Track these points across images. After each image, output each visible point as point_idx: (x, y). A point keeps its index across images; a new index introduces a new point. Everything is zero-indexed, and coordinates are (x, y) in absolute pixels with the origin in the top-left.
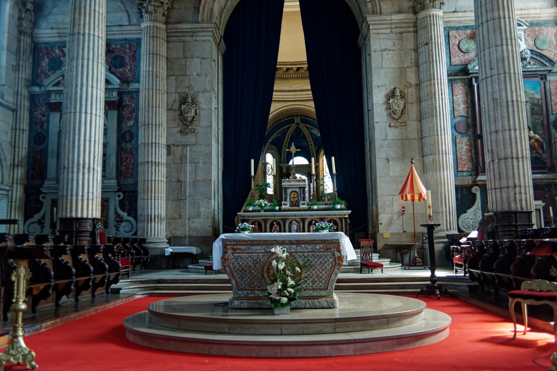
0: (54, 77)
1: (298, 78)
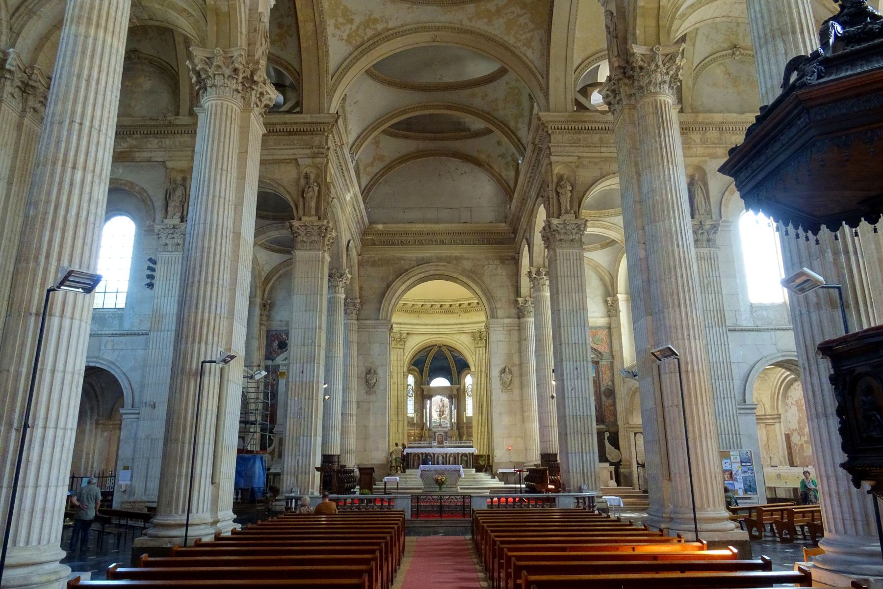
0: (283, 356)
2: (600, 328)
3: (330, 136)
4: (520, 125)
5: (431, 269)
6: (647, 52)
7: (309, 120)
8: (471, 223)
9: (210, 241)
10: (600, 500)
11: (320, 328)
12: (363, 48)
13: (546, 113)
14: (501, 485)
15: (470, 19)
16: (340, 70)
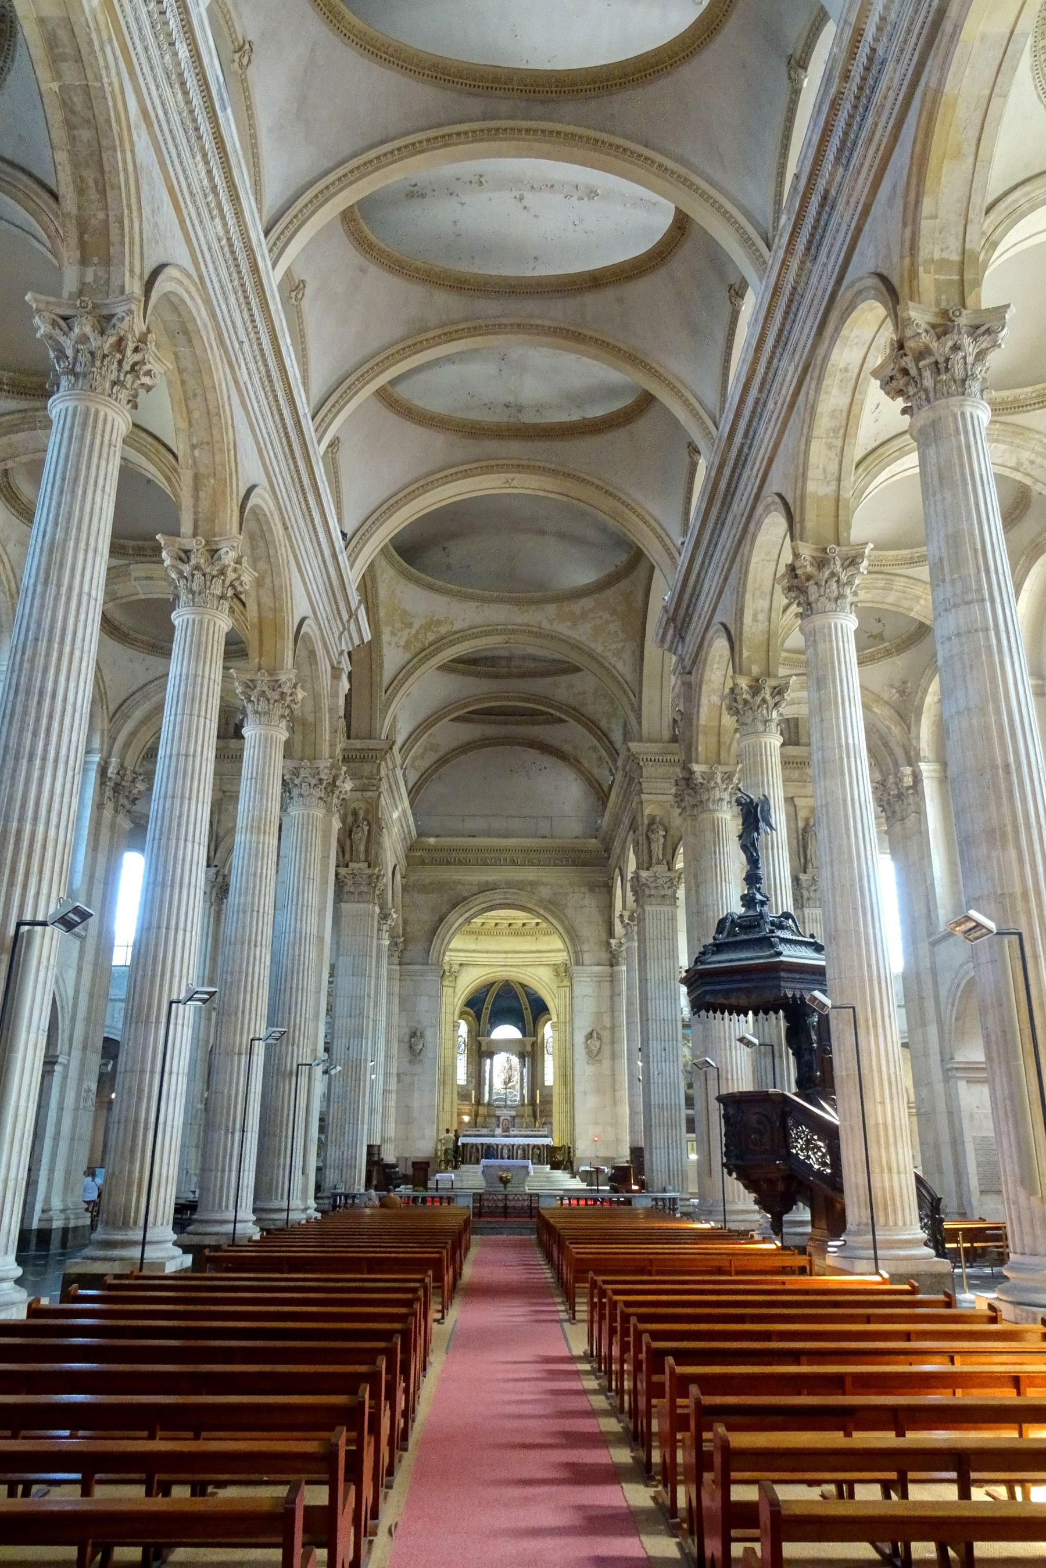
1: (510, 934)
3: (383, 763)
4: (614, 726)
5: (497, 897)
7: (358, 746)
8: (552, 837)
9: (300, 949)
10: (687, 1203)
11: (369, 996)
12: (422, 655)
14: (583, 1186)
15: (551, 622)
16: (396, 682)
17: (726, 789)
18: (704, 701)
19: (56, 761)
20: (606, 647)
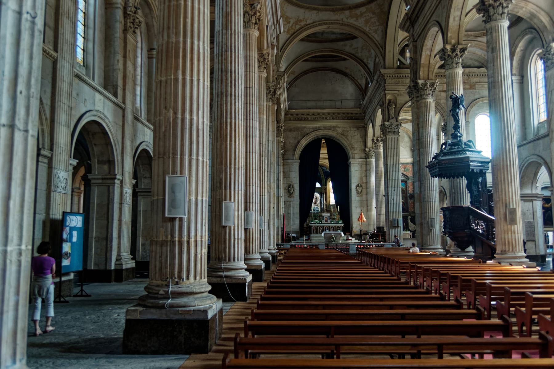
2: (408, 163)
4: (369, 62)
6: (424, 82)
12: (294, 35)
13: (384, 70)
15: (347, 18)
16: (284, 47)
17: (431, 90)
18: (424, 53)
19: (238, 96)
20: (370, 29)
